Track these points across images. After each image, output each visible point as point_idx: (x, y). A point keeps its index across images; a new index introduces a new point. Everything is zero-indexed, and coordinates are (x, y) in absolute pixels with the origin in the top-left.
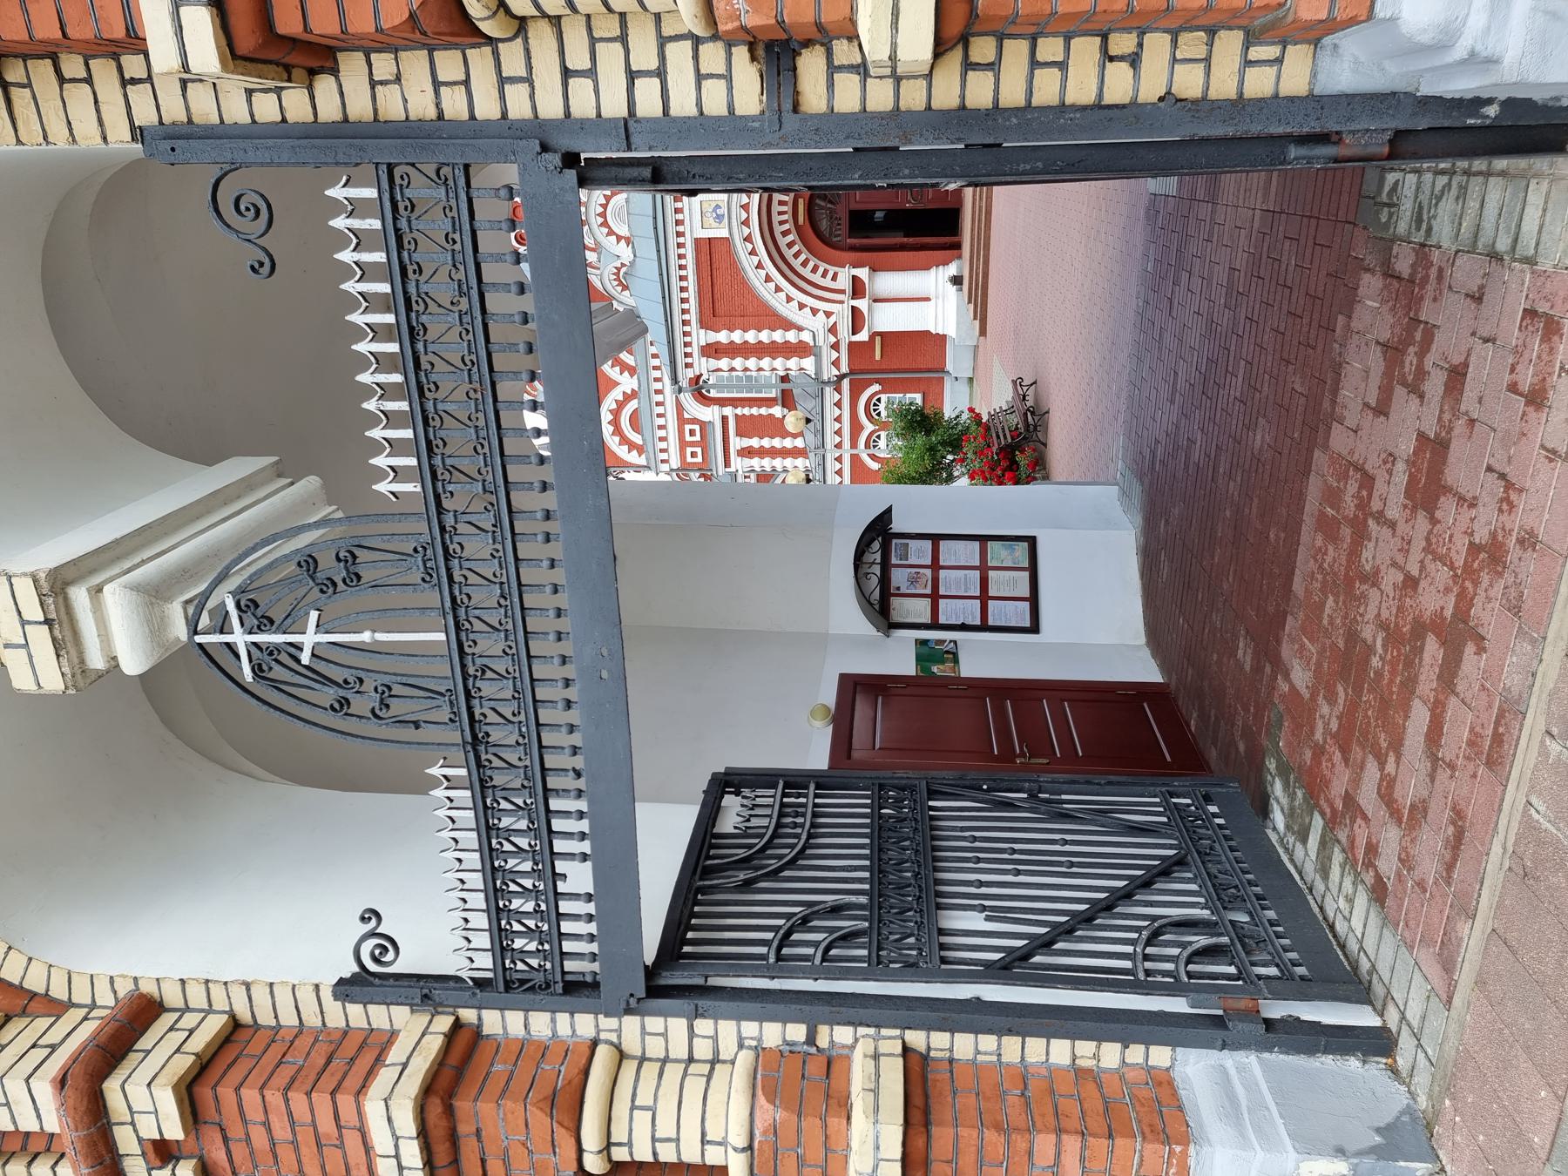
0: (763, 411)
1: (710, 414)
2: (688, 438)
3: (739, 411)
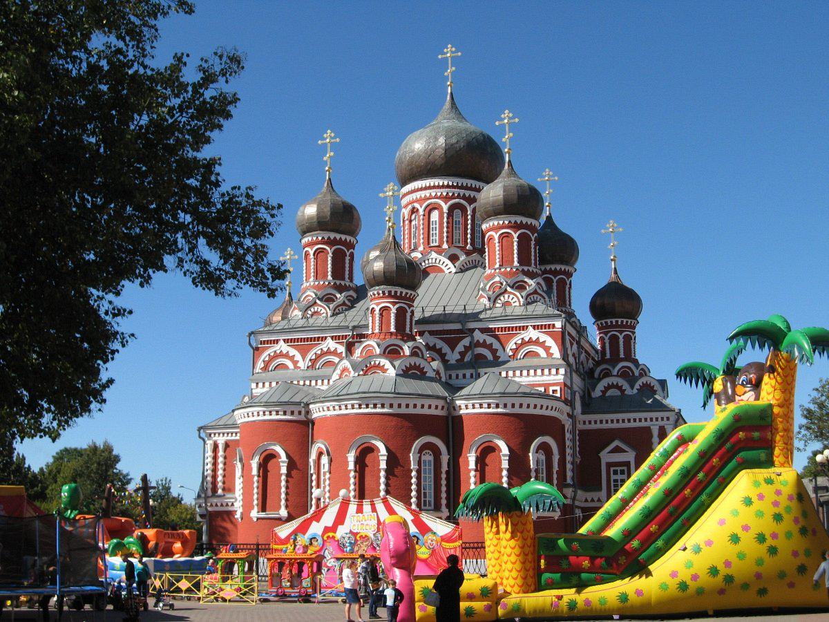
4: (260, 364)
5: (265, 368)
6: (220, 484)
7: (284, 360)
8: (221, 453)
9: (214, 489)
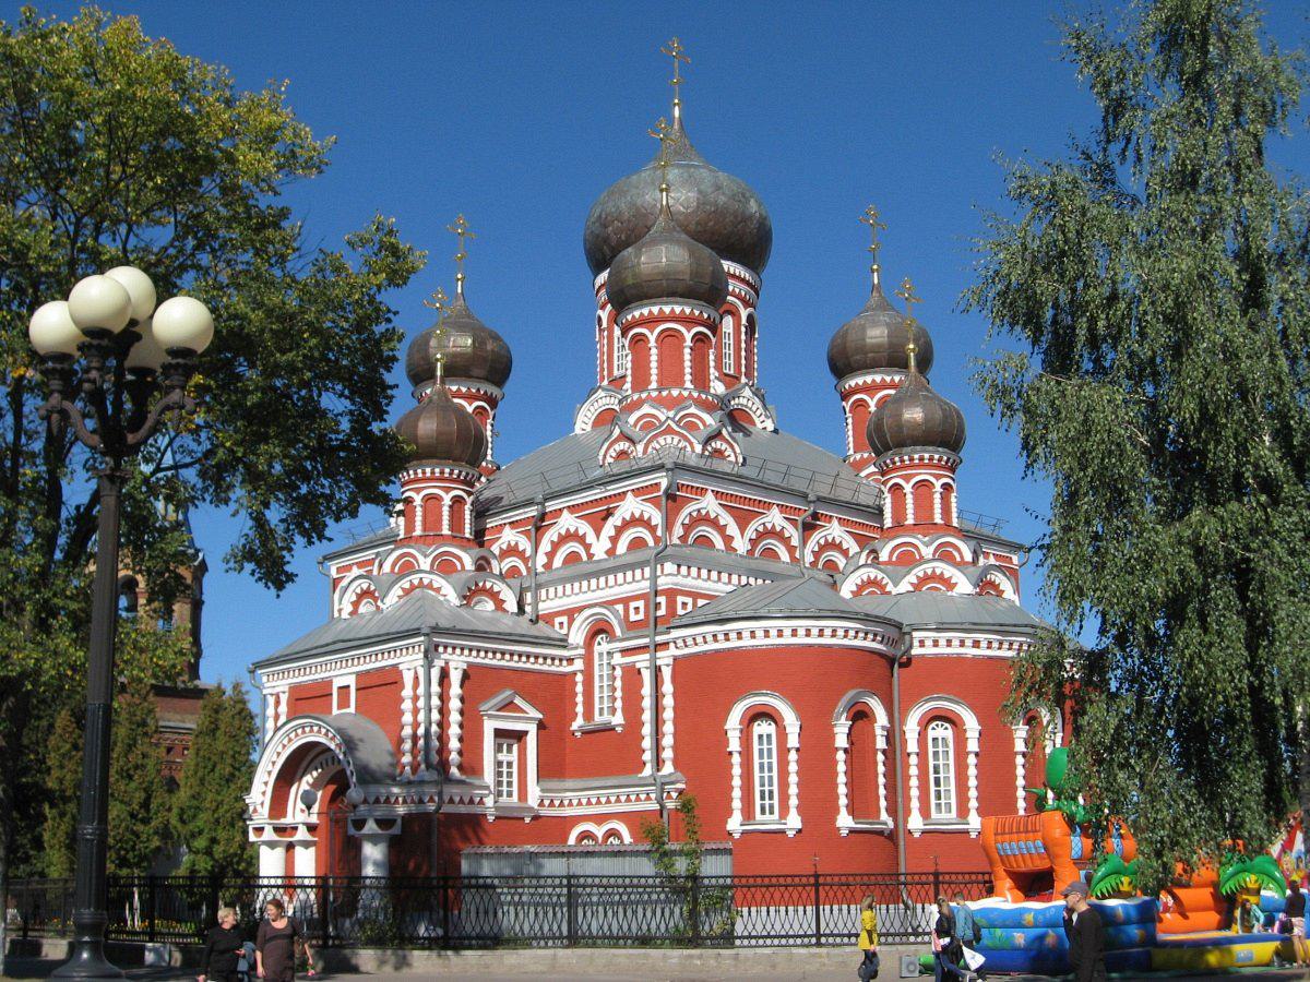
0: (580, 709)
1: (577, 636)
2: (633, 605)
3: (579, 678)
4: (678, 531)
5: (683, 538)
6: (454, 757)
7: (715, 533)
8: (455, 690)
9: (444, 765)
